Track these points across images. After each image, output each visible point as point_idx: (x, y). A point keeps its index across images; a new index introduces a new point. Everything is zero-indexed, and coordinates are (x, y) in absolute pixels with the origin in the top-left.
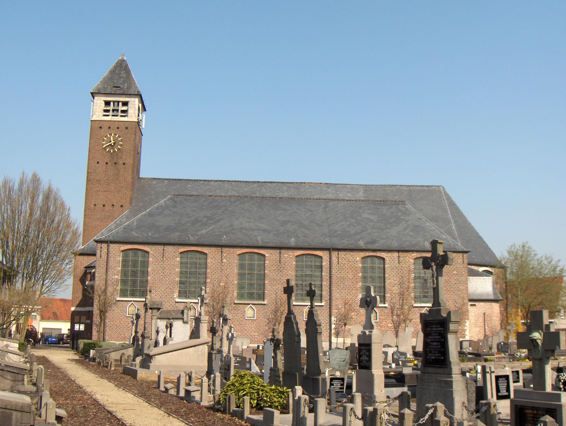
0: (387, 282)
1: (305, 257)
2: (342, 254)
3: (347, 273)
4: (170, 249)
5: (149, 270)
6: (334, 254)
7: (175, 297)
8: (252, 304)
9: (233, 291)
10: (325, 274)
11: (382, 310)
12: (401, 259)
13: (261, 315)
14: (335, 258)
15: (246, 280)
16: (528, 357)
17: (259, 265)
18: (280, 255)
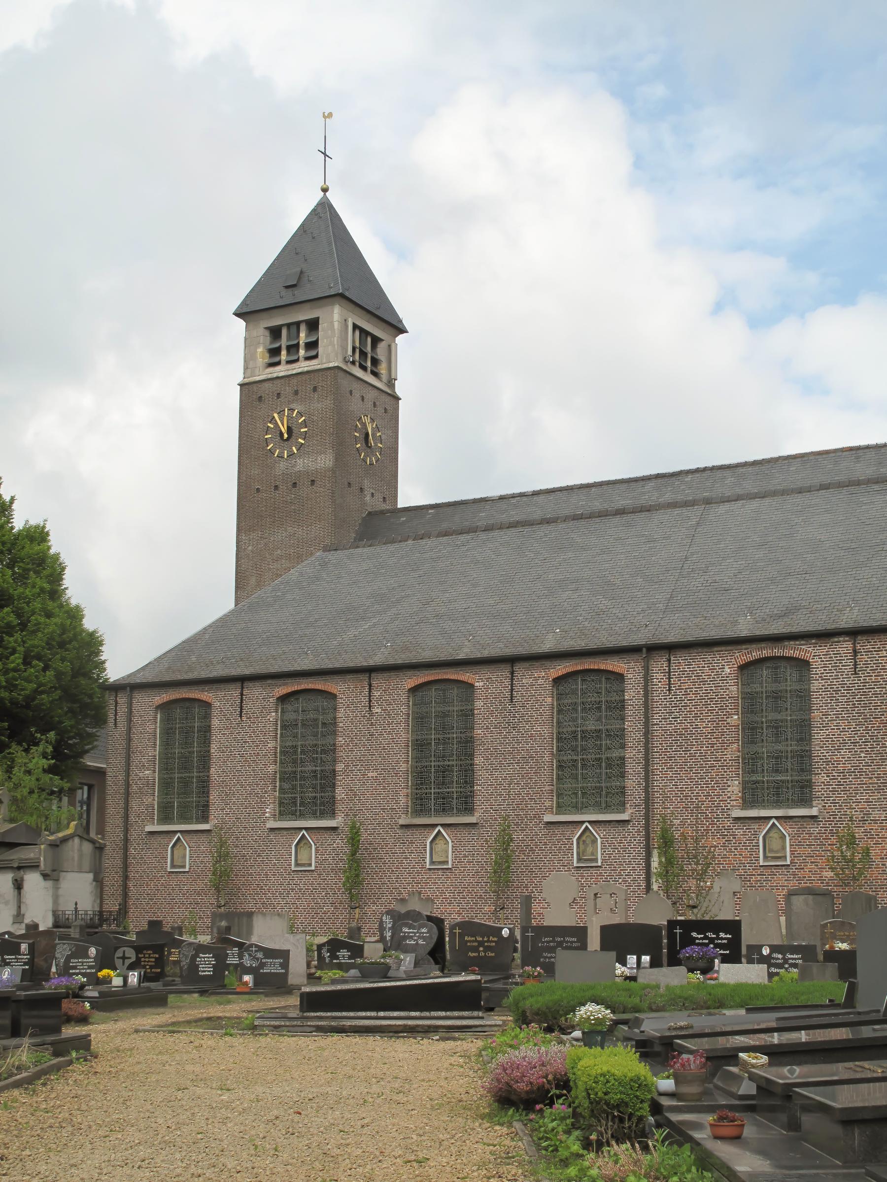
0: (819, 735)
1: (583, 680)
2: (680, 661)
3: (696, 717)
4: (255, 693)
5: (212, 751)
6: (659, 665)
7: (267, 815)
8: (442, 825)
9: (397, 793)
10: (633, 726)
11: (802, 827)
12: (863, 658)
13: (465, 856)
14: (660, 676)
15: (433, 759)
16: (782, 959)
17: (462, 715)
18: (512, 679)
